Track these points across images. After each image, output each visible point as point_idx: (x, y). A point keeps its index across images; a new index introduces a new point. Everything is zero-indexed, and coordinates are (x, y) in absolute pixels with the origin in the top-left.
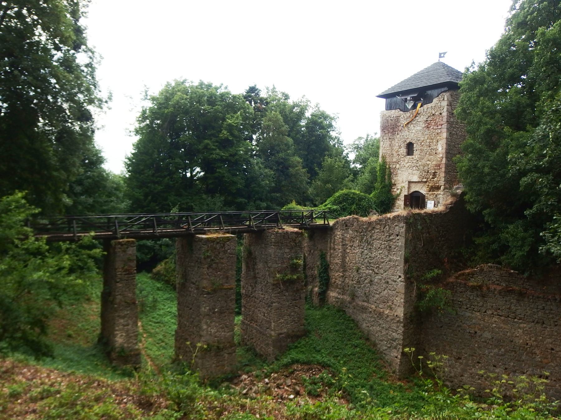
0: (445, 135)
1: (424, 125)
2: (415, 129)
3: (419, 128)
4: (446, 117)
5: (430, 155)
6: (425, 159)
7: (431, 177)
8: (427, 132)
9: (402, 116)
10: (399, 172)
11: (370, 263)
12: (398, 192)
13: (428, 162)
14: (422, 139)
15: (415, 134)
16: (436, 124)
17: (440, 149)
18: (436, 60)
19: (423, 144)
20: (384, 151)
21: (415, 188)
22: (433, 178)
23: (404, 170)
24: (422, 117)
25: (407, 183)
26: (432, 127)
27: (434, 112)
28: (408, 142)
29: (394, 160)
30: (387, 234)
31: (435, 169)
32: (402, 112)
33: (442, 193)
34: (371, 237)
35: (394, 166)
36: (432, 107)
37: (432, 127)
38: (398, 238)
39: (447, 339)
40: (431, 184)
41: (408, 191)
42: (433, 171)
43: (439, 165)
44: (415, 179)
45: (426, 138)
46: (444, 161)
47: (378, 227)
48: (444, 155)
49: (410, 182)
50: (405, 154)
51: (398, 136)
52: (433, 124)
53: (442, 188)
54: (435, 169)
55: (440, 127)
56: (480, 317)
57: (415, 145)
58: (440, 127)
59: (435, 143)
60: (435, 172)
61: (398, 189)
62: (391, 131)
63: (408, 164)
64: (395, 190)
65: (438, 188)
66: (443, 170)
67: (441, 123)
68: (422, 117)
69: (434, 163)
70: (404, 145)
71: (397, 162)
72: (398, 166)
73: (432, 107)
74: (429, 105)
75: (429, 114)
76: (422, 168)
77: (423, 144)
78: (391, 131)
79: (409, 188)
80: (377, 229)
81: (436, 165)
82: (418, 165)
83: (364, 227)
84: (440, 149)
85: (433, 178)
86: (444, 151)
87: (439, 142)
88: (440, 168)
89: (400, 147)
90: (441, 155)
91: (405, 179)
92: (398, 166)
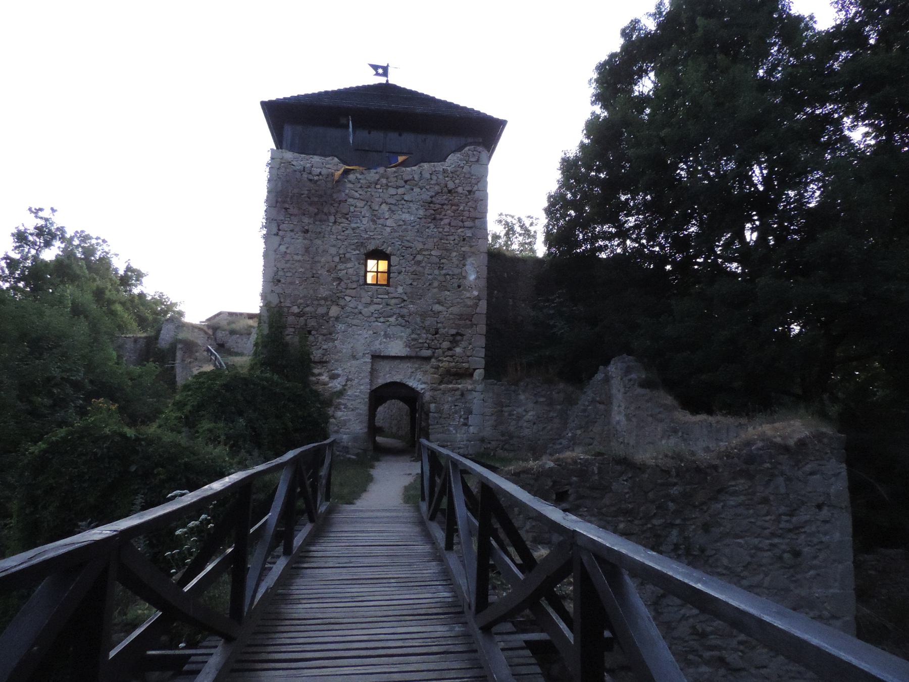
1: (421, 212)
2: (394, 217)
3: (406, 216)
5: (442, 288)
7: (446, 345)
8: (432, 230)
10: (340, 327)
11: (703, 635)
12: (337, 385)
13: (437, 308)
14: (420, 246)
15: (394, 230)
17: (472, 277)
19: (419, 258)
21: (389, 375)
23: (355, 322)
24: (417, 190)
26: (446, 221)
27: (451, 185)
29: (323, 292)
30: (783, 509)
33: (480, 387)
34: (706, 528)
37: (446, 221)
38: (825, 513)
40: (445, 364)
42: (453, 331)
43: (470, 317)
44: (397, 348)
45: (430, 245)
46: (483, 306)
47: (742, 484)
48: (485, 293)
49: (377, 357)
51: (335, 229)
53: (479, 374)
58: (467, 224)
60: (458, 334)
61: (333, 377)
63: (372, 308)
66: (482, 328)
68: (417, 190)
69: (455, 310)
71: (335, 299)
72: (334, 311)
73: (444, 171)
74: (440, 166)
75: (437, 188)
76: (418, 319)
78: (313, 210)
79: (373, 373)
80: (735, 493)
81: (461, 317)
82: (405, 311)
83: (675, 491)
84: (472, 277)
85: (450, 349)
86: (483, 283)
87: (469, 261)
88: (472, 326)
90: (476, 293)
92: (334, 311)
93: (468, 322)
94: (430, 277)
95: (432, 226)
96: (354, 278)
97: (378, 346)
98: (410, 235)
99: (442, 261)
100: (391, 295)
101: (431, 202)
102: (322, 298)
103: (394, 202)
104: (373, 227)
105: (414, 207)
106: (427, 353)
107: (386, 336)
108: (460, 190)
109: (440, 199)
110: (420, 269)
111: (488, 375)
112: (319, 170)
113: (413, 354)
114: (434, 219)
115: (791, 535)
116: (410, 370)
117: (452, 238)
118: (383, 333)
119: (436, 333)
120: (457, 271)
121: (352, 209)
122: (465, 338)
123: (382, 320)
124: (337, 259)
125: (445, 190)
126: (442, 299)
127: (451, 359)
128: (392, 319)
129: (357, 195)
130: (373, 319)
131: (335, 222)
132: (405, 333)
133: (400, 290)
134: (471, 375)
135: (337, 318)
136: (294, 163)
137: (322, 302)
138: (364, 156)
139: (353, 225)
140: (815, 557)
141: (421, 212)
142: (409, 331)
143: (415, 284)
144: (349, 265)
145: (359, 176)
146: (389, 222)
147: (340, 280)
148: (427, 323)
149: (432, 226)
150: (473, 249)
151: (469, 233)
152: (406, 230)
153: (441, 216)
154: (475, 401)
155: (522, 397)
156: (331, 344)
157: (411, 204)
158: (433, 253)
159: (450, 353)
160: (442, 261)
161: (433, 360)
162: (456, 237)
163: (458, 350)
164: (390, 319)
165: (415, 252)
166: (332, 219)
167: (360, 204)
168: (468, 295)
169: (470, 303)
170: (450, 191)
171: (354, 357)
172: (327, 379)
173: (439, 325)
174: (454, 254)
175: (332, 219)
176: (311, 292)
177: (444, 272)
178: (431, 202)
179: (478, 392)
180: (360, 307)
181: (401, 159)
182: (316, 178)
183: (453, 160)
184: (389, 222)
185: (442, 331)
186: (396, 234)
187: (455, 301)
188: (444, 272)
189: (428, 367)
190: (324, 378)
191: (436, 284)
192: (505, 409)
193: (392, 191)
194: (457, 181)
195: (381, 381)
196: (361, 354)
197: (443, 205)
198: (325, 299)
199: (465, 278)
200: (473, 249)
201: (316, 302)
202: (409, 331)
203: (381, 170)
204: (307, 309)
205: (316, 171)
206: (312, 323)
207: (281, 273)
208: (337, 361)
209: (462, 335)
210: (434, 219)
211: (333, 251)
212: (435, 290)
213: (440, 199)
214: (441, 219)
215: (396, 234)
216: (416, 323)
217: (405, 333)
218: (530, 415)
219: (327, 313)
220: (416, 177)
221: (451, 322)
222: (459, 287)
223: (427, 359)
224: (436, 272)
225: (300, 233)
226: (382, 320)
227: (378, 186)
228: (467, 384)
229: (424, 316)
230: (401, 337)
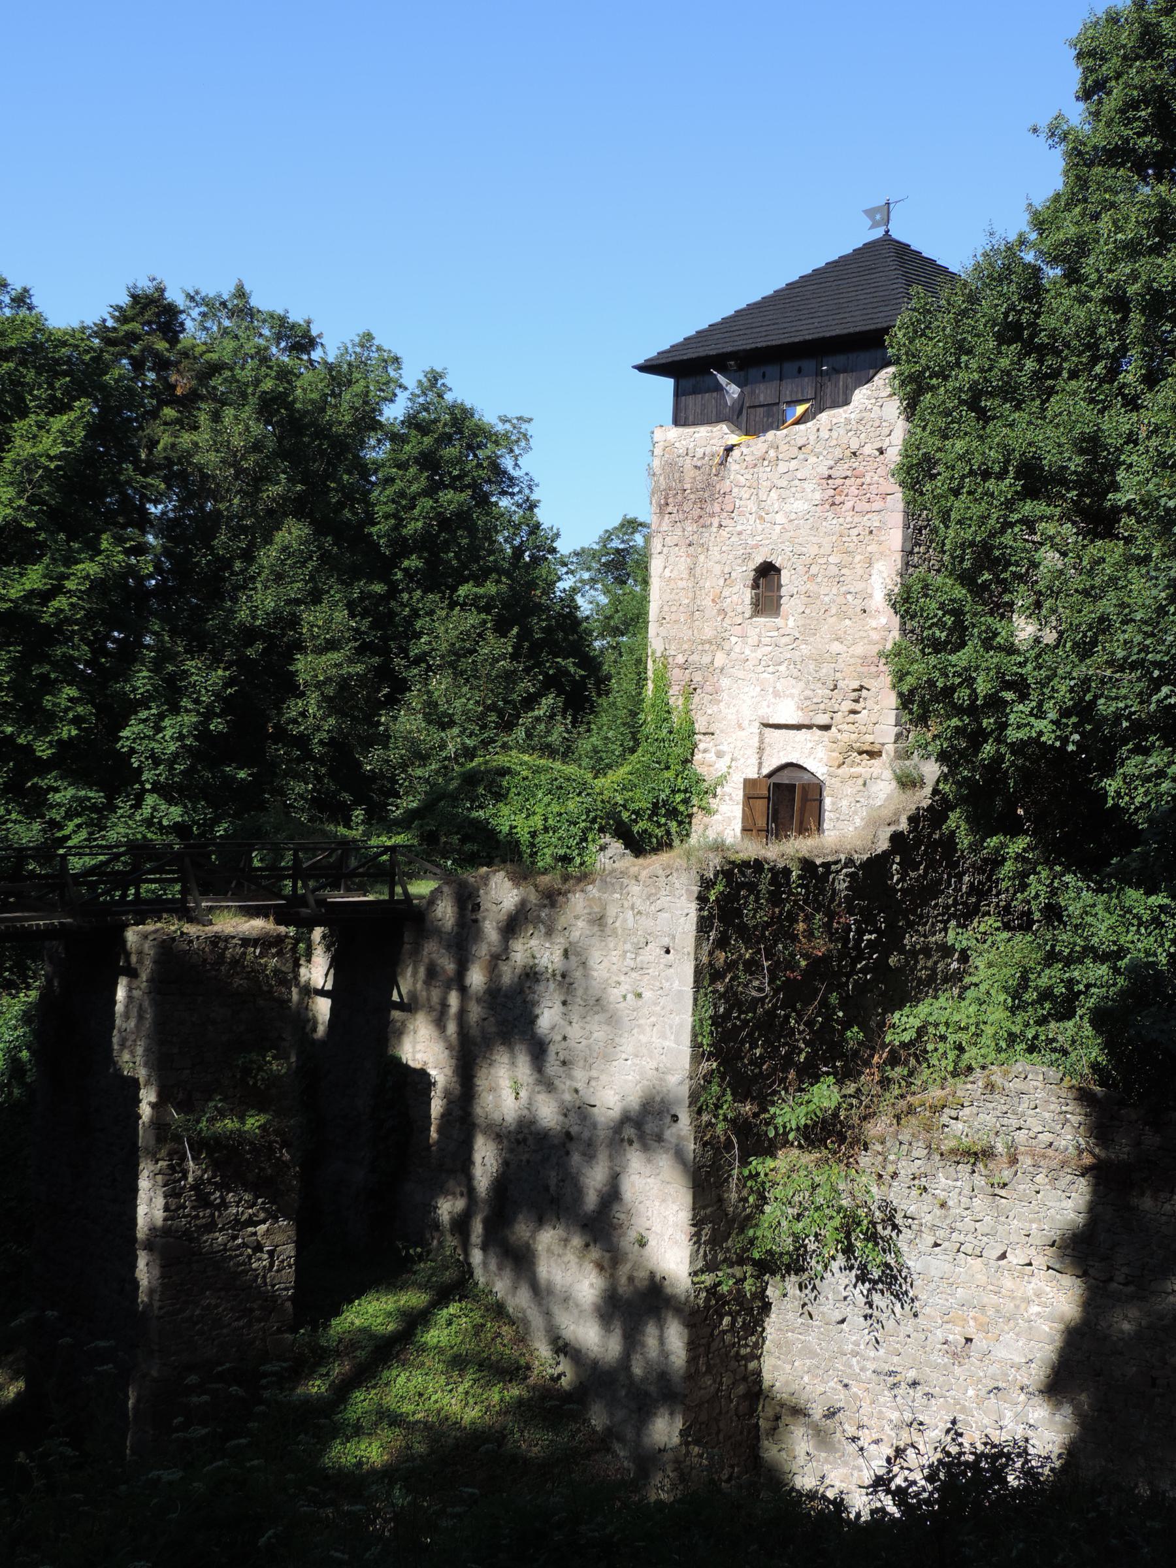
0: (895, 538)
1: (818, 496)
2: (787, 508)
3: (800, 506)
5: (842, 615)
7: (848, 705)
8: (832, 524)
10: (725, 682)
12: (721, 766)
13: (836, 647)
14: (814, 550)
15: (784, 530)
20: (666, 597)
25: (755, 728)
26: (849, 505)
28: (759, 560)
29: (708, 633)
31: (860, 676)
35: (706, 659)
36: (848, 421)
37: (849, 505)
39: (863, 1369)
42: (856, 685)
52: (853, 490)
54: (860, 676)
56: (981, 1279)
57: (785, 575)
58: (876, 506)
59: (860, 572)
61: (720, 755)
62: (697, 512)
64: (711, 757)
69: (859, 650)
70: (745, 573)
71: (718, 642)
72: (720, 659)
75: (838, 453)
77: (814, 569)
94: (827, 599)
96: (740, 609)
99: (843, 572)
101: (830, 477)
104: (760, 528)
105: (809, 486)
106: (823, 719)
107: (776, 694)
110: (816, 587)
112: (702, 450)
115: (634, 975)
116: (810, 745)
117: (855, 532)
118: (771, 690)
120: (860, 586)
123: (771, 669)
128: (782, 668)
130: (760, 669)
132: (796, 689)
133: (791, 623)
136: (677, 445)
138: (755, 419)
139: (739, 528)
140: (656, 1004)
142: (801, 685)
146: (780, 518)
152: (798, 528)
156: (715, 708)
157: (805, 485)
158: (831, 559)
160: (843, 571)
161: (833, 729)
168: (874, 624)
171: (740, 727)
173: (838, 674)
174: (858, 558)
178: (830, 477)
180: (747, 652)
181: (800, 409)
184: (780, 518)
185: (840, 684)
188: (843, 589)
190: (711, 757)
191: (833, 611)
193: (782, 467)
197: (845, 478)
201: (700, 647)
202: (801, 685)
207: (666, 608)
208: (722, 731)
210: (833, 504)
212: (834, 619)
216: (809, 674)
217: (796, 689)
226: (771, 669)
227: (766, 463)
229: (819, 660)
230: (792, 696)
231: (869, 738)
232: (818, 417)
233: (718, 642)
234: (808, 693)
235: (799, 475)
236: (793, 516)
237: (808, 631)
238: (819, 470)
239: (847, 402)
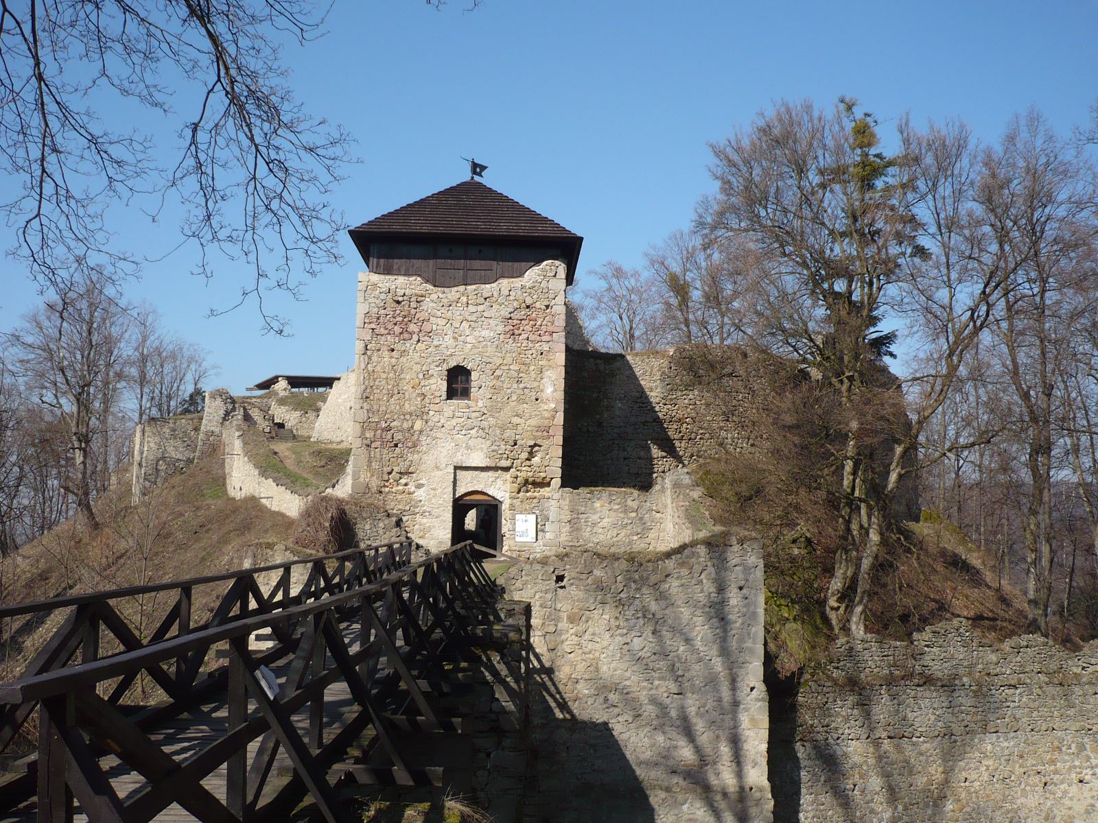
1: (500, 328)
2: (476, 333)
3: (486, 333)
4: (563, 317)
5: (520, 401)
6: (507, 409)
7: (525, 455)
8: (511, 345)
9: (434, 297)
13: (516, 420)
14: (499, 361)
15: (474, 347)
16: (536, 329)
17: (549, 390)
18: (465, 175)
19: (498, 373)
21: (468, 483)
22: (528, 459)
26: (524, 336)
27: (529, 301)
28: (453, 364)
29: (408, 407)
31: (535, 438)
32: (429, 287)
35: (405, 425)
36: (523, 287)
37: (524, 336)
40: (522, 475)
41: (454, 494)
42: (532, 443)
44: (478, 459)
45: (508, 360)
48: (561, 407)
50: (444, 396)
52: (528, 328)
53: (557, 482)
55: (546, 338)
57: (474, 376)
58: (546, 338)
59: (533, 375)
60: (536, 445)
62: (397, 329)
63: (454, 422)
65: (544, 484)
66: (559, 439)
67: (550, 329)
69: (533, 422)
72: (418, 425)
73: (523, 287)
74: (517, 282)
75: (516, 304)
76: (498, 432)
77: (498, 373)
82: (485, 424)
84: (549, 390)
85: (528, 459)
86: (560, 395)
89: (427, 375)
90: (554, 406)
91: (444, 461)
93: (545, 434)
94: (509, 391)
95: (511, 341)
96: (438, 394)
97: (460, 457)
98: (491, 349)
99: (521, 375)
100: (474, 409)
101: (510, 318)
102: (407, 414)
103: (474, 319)
104: (454, 344)
106: (504, 463)
107: (468, 447)
108: (538, 305)
109: (516, 315)
110: (499, 383)
111: (563, 486)
112: (403, 291)
113: (493, 465)
114: (513, 334)
119: (515, 444)
121: (434, 328)
122: (542, 448)
123: (463, 432)
124: (421, 376)
125: (524, 305)
126: (520, 412)
127: (529, 469)
129: (439, 314)
130: (455, 432)
131: (419, 341)
133: (480, 404)
134: (548, 484)
135: (421, 432)
137: (408, 417)
139: (436, 343)
141: (500, 328)
142: (489, 443)
143: (494, 397)
144: (431, 381)
145: (441, 296)
146: (469, 339)
147: (424, 395)
148: (505, 436)
149: (511, 341)
150: (550, 363)
151: (546, 347)
153: (520, 332)
154: (552, 508)
155: (597, 505)
157: (491, 321)
159: (528, 463)
160: (521, 375)
162: (534, 351)
163: (536, 460)
164: (471, 432)
165: (494, 367)
166: (415, 337)
167: (442, 322)
168: (546, 407)
169: (546, 415)
170: (528, 307)
171: (437, 468)
172: (413, 489)
174: (532, 368)
175: (415, 337)
176: (398, 407)
177: (522, 386)
178: (510, 318)
179: (556, 499)
182: (400, 299)
183: (533, 274)
184: (469, 339)
186: (476, 351)
187: (533, 413)
188: (522, 386)
189: (508, 476)
191: (514, 397)
192: (581, 516)
193: (472, 308)
194: (535, 297)
195: (461, 491)
196: (444, 465)
198: (411, 414)
199: (542, 391)
200: (550, 363)
201: (402, 417)
203: (462, 288)
204: (393, 424)
205: (400, 292)
206: (398, 436)
209: (540, 446)
210: (513, 334)
211: (417, 368)
213: (516, 315)
214: (520, 335)
215: (476, 351)
218: (605, 522)
219: (412, 427)
220: (496, 294)
221: (529, 433)
222: (537, 400)
223: (507, 469)
224: (515, 386)
225: (386, 352)
226: (463, 432)
227: (459, 305)
228: (545, 491)
230: (482, 449)
231: (543, 475)
232: (500, 281)
233: (422, 414)
234: (494, 447)
235: (486, 314)
236: (481, 339)
237: (494, 409)
238: (502, 313)
239: (521, 275)
